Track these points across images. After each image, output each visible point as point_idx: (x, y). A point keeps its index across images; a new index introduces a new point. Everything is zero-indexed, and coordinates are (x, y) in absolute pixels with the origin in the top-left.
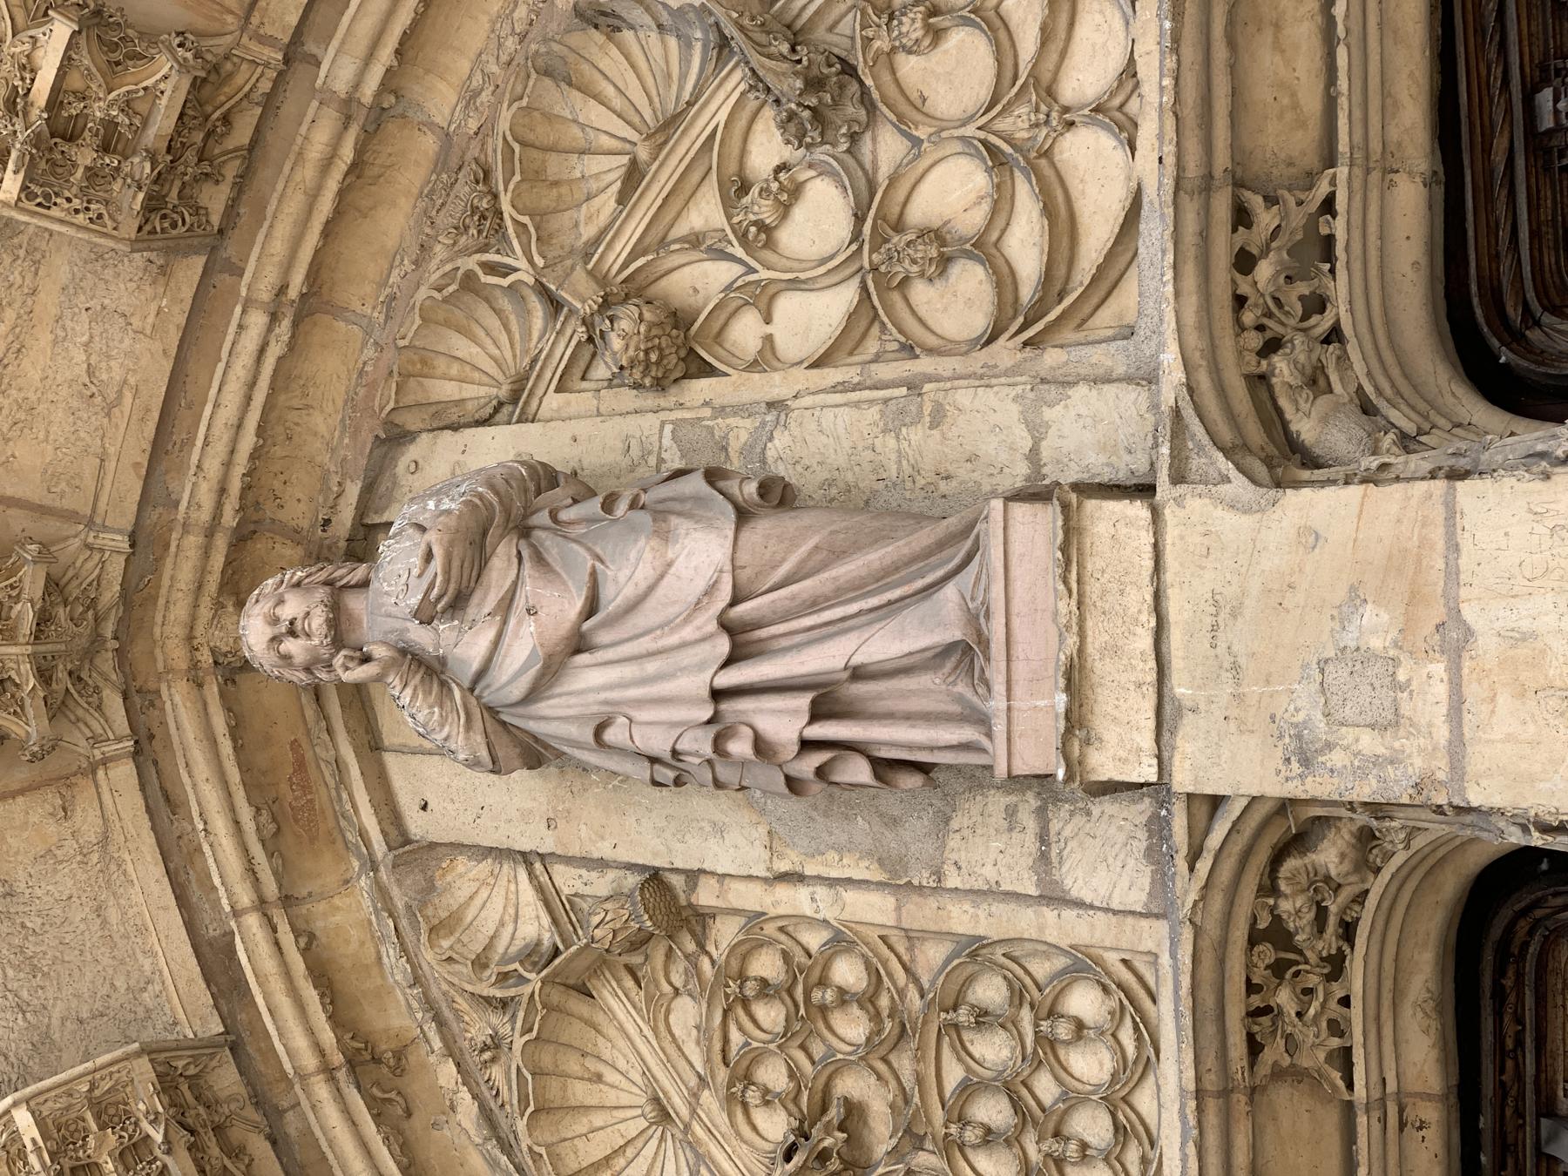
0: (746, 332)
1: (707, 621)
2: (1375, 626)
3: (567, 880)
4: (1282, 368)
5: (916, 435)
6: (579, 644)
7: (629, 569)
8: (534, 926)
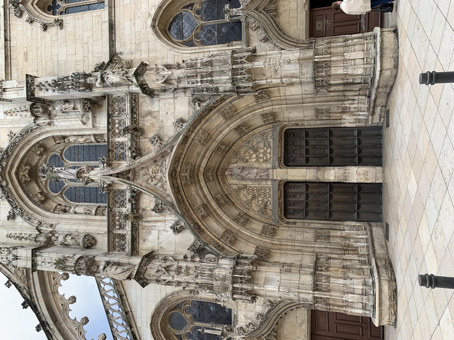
0: (250, 160)
2: (285, 174)
3: (239, 185)
7: (251, 171)
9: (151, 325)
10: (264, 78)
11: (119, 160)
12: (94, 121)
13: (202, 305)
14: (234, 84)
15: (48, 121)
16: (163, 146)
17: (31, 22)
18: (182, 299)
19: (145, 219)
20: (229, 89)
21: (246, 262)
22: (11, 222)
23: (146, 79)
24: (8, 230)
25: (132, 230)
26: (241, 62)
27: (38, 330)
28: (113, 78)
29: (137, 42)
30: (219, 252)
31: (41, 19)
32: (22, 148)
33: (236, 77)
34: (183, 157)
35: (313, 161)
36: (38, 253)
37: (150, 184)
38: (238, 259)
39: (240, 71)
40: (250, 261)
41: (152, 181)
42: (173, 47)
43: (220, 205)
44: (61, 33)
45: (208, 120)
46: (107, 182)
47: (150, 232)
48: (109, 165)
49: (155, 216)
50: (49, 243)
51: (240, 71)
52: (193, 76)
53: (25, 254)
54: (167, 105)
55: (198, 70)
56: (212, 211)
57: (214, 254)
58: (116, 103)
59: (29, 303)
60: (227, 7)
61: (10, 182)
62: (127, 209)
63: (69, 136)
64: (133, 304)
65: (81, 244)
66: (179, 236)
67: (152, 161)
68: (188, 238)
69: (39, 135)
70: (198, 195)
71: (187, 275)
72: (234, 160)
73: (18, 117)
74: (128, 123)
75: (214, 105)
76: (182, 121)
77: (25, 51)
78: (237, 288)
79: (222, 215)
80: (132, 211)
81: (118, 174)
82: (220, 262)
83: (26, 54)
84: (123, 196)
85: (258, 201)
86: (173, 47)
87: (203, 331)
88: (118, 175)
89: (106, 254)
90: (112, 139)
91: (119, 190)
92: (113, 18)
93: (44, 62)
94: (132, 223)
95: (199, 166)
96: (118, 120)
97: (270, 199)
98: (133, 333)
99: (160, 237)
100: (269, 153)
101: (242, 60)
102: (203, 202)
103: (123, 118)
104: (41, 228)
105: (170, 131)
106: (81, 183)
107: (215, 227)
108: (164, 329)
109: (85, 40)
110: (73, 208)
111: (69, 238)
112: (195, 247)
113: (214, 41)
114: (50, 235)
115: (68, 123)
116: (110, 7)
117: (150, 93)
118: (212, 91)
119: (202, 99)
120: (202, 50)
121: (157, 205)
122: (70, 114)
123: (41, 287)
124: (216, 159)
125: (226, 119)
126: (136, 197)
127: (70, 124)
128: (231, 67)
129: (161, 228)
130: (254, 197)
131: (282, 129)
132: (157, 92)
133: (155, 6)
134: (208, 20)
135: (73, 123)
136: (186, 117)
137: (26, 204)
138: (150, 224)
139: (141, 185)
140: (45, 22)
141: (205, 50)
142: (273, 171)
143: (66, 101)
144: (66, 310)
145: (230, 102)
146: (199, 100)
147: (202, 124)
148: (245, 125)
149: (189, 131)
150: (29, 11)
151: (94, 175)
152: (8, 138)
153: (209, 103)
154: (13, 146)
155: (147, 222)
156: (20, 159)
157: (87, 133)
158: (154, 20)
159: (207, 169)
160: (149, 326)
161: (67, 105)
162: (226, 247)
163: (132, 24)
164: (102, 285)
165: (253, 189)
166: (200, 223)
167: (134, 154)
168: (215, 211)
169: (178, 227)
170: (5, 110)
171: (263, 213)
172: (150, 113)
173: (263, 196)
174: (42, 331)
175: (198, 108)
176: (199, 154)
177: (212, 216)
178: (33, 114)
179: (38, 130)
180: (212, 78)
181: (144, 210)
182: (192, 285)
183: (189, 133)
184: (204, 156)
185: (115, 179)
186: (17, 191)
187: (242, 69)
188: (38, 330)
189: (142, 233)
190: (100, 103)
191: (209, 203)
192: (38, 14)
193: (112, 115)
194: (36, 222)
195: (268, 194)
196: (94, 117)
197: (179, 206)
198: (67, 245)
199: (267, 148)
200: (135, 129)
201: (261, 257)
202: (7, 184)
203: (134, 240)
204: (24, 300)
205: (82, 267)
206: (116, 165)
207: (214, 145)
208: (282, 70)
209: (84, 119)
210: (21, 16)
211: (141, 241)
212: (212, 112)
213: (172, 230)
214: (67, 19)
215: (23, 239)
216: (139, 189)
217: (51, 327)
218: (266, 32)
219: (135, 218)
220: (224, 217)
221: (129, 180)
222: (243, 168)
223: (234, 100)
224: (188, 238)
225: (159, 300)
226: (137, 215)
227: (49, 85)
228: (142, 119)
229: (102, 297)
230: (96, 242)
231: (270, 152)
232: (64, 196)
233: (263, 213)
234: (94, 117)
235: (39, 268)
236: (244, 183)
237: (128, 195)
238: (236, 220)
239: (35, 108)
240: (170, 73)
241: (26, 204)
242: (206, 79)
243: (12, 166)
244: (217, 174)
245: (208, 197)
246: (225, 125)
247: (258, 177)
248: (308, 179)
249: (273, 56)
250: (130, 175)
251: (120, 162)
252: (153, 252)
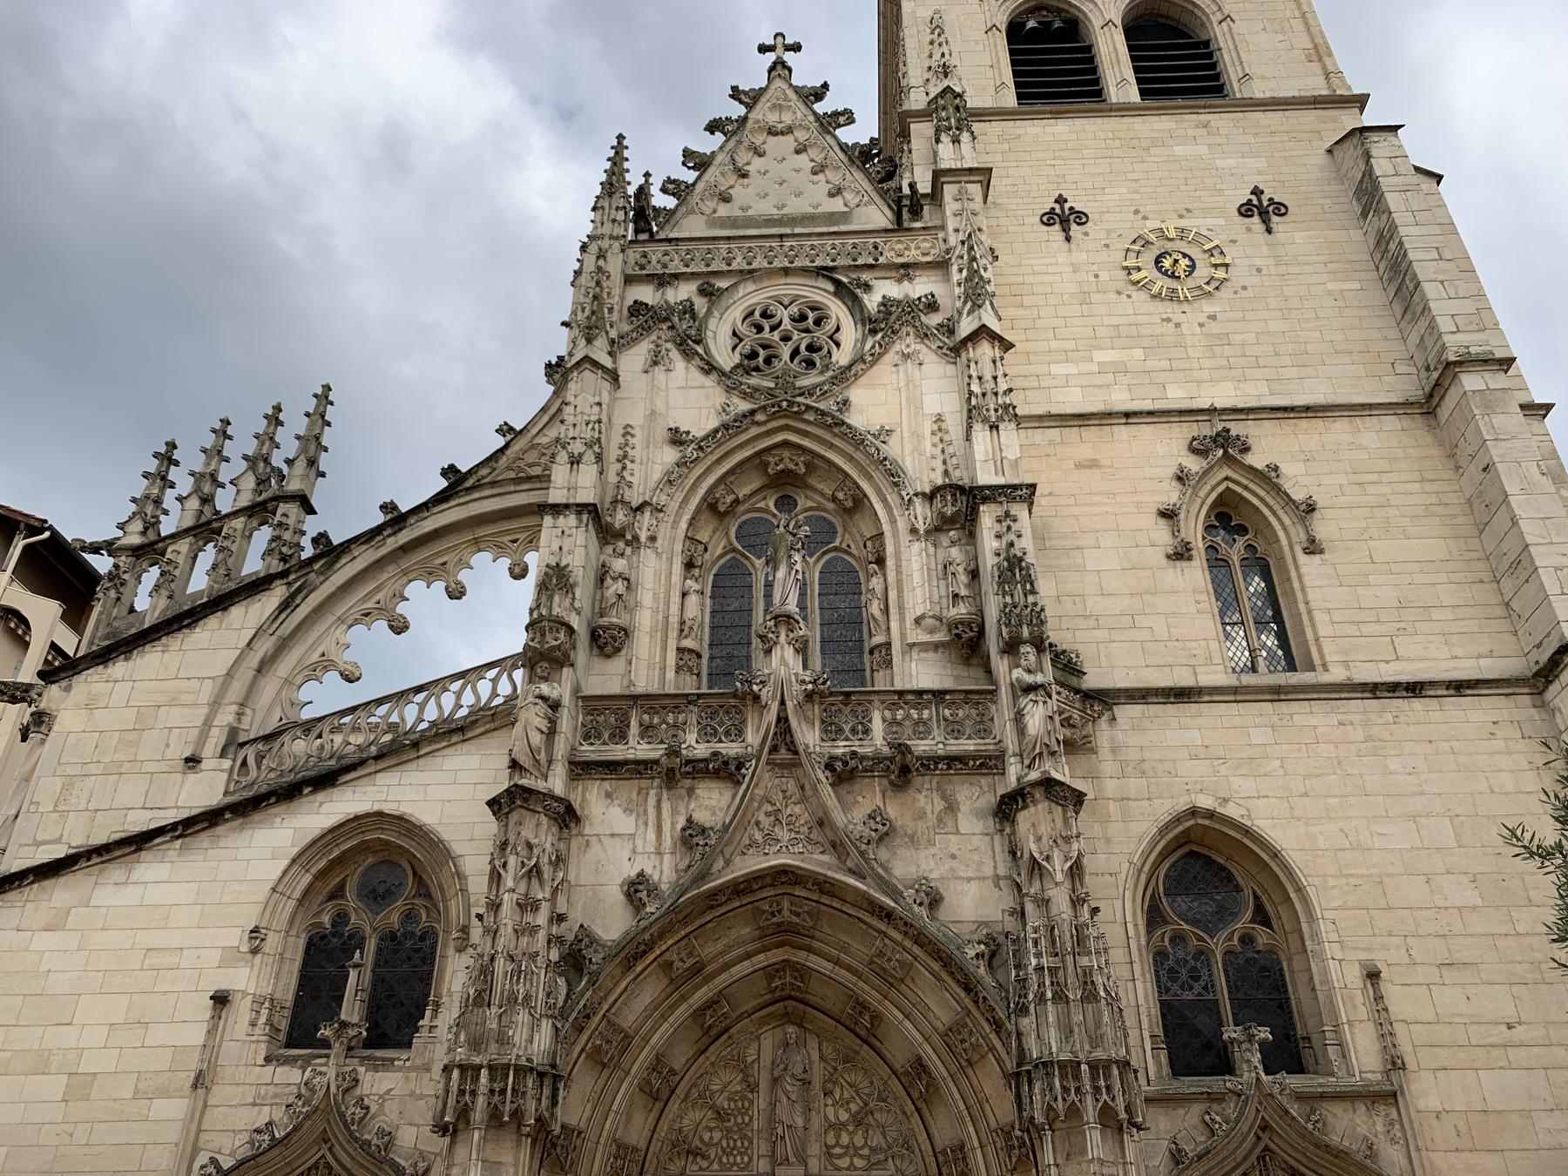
7: (798, 1108)
8: (750, 1059)
9: (380, 814)
10: (1059, 1156)
11: (823, 722)
12: (924, 647)
13: (423, 960)
14: (1036, 1066)
15: (922, 528)
17: (1180, 479)
18: (445, 901)
19: (665, 796)
21: (545, 1102)
22: (661, 434)
23: (1040, 806)
24: (642, 427)
25: (637, 762)
26: (1097, 1089)
27: (384, 507)
28: (1037, 718)
29: (1146, 766)
31: (1189, 504)
32: (851, 459)
36: (585, 517)
37: (759, 808)
38: (551, 1077)
39: (1072, 1085)
40: (546, 1115)
41: (768, 814)
42: (1140, 871)
43: (700, 1013)
44: (1157, 557)
45: (939, 979)
46: (765, 690)
47: (631, 811)
48: (809, 696)
49: (673, 824)
50: (607, 534)
51: (1072, 1085)
52: (1053, 942)
53: (584, 485)
54: (976, 857)
55: (1070, 959)
56: (683, 990)
57: (566, 1001)
58: (974, 712)
59: (457, 482)
60: (1264, 1033)
61: (763, 429)
62: (695, 746)
63: (884, 575)
64: (437, 761)
65: (604, 621)
66: (614, 895)
67: (821, 814)
68: (612, 922)
69: (884, 501)
70: (729, 948)
71: (516, 931)
72: (828, 1050)
73: (929, 450)
74: (921, 746)
76: (934, 901)
77: (1103, 462)
78: (478, 1079)
79: (671, 1019)
80: (688, 762)
81: (787, 720)
82: (544, 1021)
83: (1093, 464)
84: (727, 733)
85: (711, 1130)
86: (1140, 871)
87: (356, 966)
88: (782, 720)
89: (576, 690)
90: (877, 703)
91: (744, 722)
92: (1207, 698)
93: (1077, 511)
94: (656, 762)
95: (810, 950)
96: (930, 719)
97: (716, 1167)
98: (362, 763)
99: (617, 839)
102: (710, 962)
103: (936, 732)
104: (647, 514)
105: (908, 865)
106: (761, 621)
107: (637, 1001)
108: (364, 847)
109: (1142, 621)
110: (697, 587)
111: (620, 587)
112: (587, 946)
113: (1168, 990)
114: (629, 537)
115: (917, 578)
116: (1235, 690)
117: (1007, 808)
119: (996, 962)
120: (1135, 957)
121: (703, 831)
122: (942, 583)
123: (494, 512)
124: (830, 998)
125: (944, 1035)
126: (726, 771)
127: (915, 583)
128: (1082, 1057)
129: (639, 842)
130: (721, 1115)
132: (1008, 830)
133: (1249, 816)
134: (1226, 971)
135: (918, 592)
136: (944, 913)
137: (708, 471)
138: (651, 811)
139: (757, 785)
140: (1182, 516)
141: (1137, 967)
143: (974, 574)
144: (430, 575)
145: (992, 1049)
146: (993, 955)
148: (932, 1090)
149: (906, 924)
150: (1206, 472)
151: (782, 657)
152: (875, 429)
153: (989, 983)
154: (857, 440)
155: (659, 801)
156: (822, 452)
157: (894, 625)
158: (1211, 814)
159: (801, 972)
160: (376, 807)
161: (963, 578)
162: (584, 1038)
163: (1194, 752)
164: (492, 673)
165: (743, 1112)
166: (651, 958)
167: (838, 765)
168: (683, 998)
169: (643, 895)
170: (947, 417)
171: (674, 1146)
172: (951, 808)
173: (724, 1143)
174: (380, 518)
175: (972, 953)
176: (844, 948)
177: (668, 990)
178: (936, 490)
179: (898, 501)
181: (691, 792)
182: (489, 944)
183: (901, 923)
184: (837, 962)
185: (772, 715)
186: (742, 446)
187: (1078, 1090)
188: (384, 507)
189: (628, 789)
190: (975, 661)
191: (706, 980)
192: (1202, 494)
193: (943, 701)
194: (663, 499)
196: (936, 646)
197: (698, 896)
198: (602, 581)
199: (868, 1158)
200: (905, 770)
201: (554, 1146)
202: (758, 424)
203: (612, 768)
204: (464, 470)
205: (548, 637)
206: (809, 713)
207: (871, 996)
209: (929, 621)
210: (1193, 450)
211: (606, 785)
212: (963, 994)
213: (633, 874)
214: (1196, 574)
215: (619, 466)
216: (747, 779)
217: (390, 541)
218: (1200, 1157)
219: (671, 771)
220: (666, 1025)
221: (770, 752)
222: (806, 1083)
223: (999, 1060)
224: (612, 922)
225: (447, 835)
226: (677, 773)
227: (1012, 544)
228: (934, 785)
229: (462, 675)
230: (608, 656)
231: (856, 1169)
232: (729, 557)
233: (674, 1146)
234: (936, 646)
235: (548, 520)
236: (764, 1086)
237: (730, 748)
238: (657, 1064)
239: (954, 495)
240: (1059, 877)
241: (708, 471)
242: (1048, 983)
243: (806, 434)
244: (789, 1000)
245: (723, 976)
246: (929, 1031)
250: (784, 754)
251: (817, 724)
252: (578, 820)
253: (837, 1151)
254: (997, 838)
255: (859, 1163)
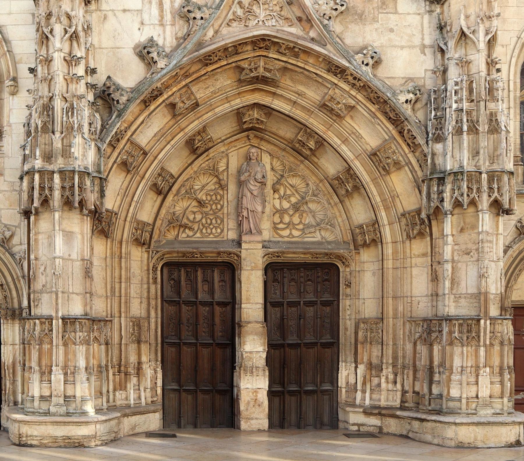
1: (254, 209)
4: (270, 256)
5: (266, 218)
6: (252, 194)
7: (258, 200)
8: (221, 169)
10: (454, 230)
16: (326, 22)
20: (437, 162)
26: (491, 189)
30: (107, 141)
33: (465, 179)
34: (299, 64)
35: (276, 313)
39: (475, 187)
51: (475, 187)
75: (406, 132)
100: (291, 234)
101: (496, 190)
118: (437, 129)
128: (483, 169)
131: (340, 257)
142: (259, 242)
147: (368, 105)
149: (355, 78)
162: (115, 154)
180: (465, 133)
183: (350, 78)
195: (209, 231)
208: (469, 263)
222: (263, 184)
223: (413, 171)
231: (294, 237)
242: (465, 120)
247: (245, 214)
248: (243, 306)
249: (494, 247)
253: (281, 226)
254: (426, 17)
255: (296, 233)
